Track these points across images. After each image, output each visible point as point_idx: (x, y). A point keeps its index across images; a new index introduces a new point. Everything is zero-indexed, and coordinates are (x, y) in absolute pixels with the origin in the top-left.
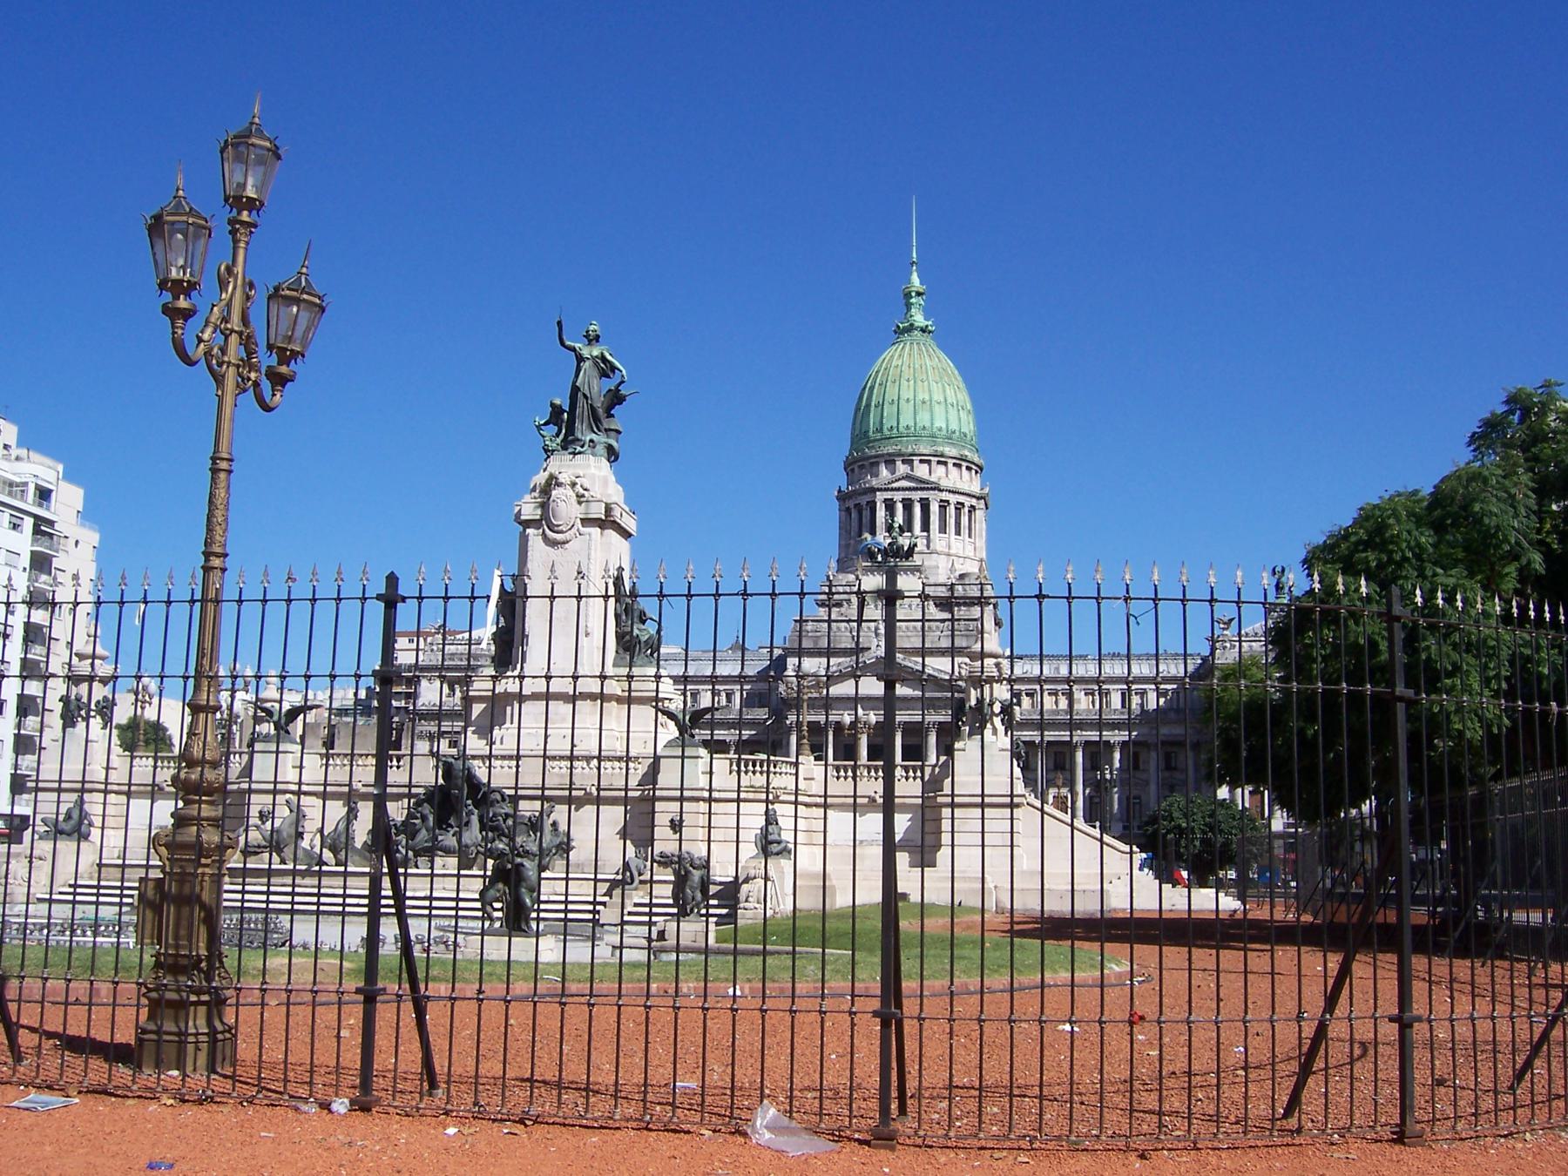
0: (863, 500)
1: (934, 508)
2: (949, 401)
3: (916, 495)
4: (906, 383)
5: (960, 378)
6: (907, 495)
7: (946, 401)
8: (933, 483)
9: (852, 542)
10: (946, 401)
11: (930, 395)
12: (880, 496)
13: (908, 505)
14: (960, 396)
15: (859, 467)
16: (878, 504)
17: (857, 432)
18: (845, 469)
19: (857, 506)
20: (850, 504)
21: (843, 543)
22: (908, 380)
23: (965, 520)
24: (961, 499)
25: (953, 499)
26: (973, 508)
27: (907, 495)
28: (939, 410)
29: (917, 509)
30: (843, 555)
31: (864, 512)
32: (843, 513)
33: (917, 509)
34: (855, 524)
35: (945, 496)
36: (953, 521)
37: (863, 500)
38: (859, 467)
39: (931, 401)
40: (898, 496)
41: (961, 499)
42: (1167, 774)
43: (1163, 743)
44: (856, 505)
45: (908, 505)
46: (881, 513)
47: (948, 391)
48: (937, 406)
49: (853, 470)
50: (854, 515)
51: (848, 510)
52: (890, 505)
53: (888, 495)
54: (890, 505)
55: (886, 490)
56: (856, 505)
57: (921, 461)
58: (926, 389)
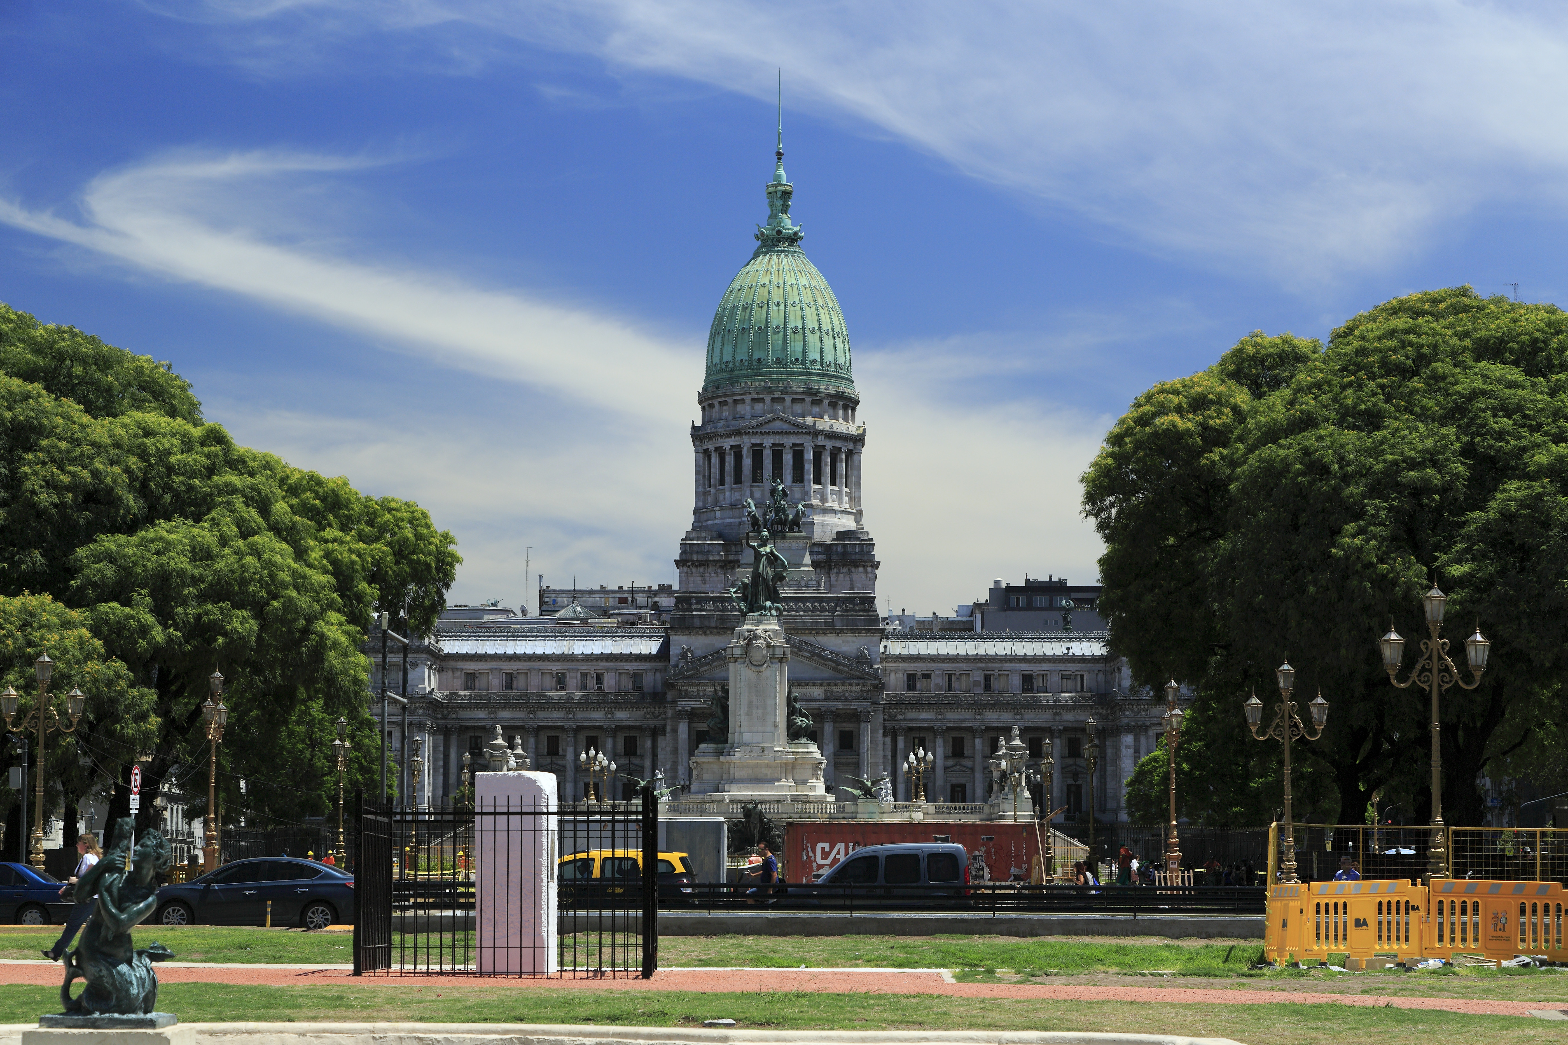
0: (727, 443)
1: (809, 455)
2: (824, 328)
3: (789, 441)
4: (775, 308)
5: (825, 281)
6: (778, 440)
7: (820, 329)
8: (807, 427)
9: (712, 490)
10: (820, 329)
11: (803, 323)
12: (747, 442)
13: (778, 456)
14: (836, 321)
15: (720, 403)
16: (745, 451)
17: (716, 360)
18: (700, 402)
19: (721, 452)
20: (711, 446)
21: (701, 489)
22: (778, 304)
23: (842, 467)
24: (838, 444)
25: (829, 444)
26: (850, 454)
27: (778, 440)
28: (813, 340)
29: (788, 458)
30: (700, 504)
31: (727, 458)
32: (701, 455)
33: (788, 458)
34: (715, 471)
35: (821, 441)
36: (828, 469)
37: (727, 443)
38: (720, 403)
39: (804, 328)
40: (768, 442)
41: (838, 444)
42: (1070, 761)
43: (1066, 729)
44: (717, 449)
45: (778, 456)
46: (747, 462)
47: (822, 315)
48: (811, 335)
49: (711, 406)
50: (715, 460)
51: (706, 453)
52: (757, 453)
53: (756, 440)
54: (757, 453)
55: (754, 433)
56: (717, 449)
57: (794, 400)
58: (799, 313)
